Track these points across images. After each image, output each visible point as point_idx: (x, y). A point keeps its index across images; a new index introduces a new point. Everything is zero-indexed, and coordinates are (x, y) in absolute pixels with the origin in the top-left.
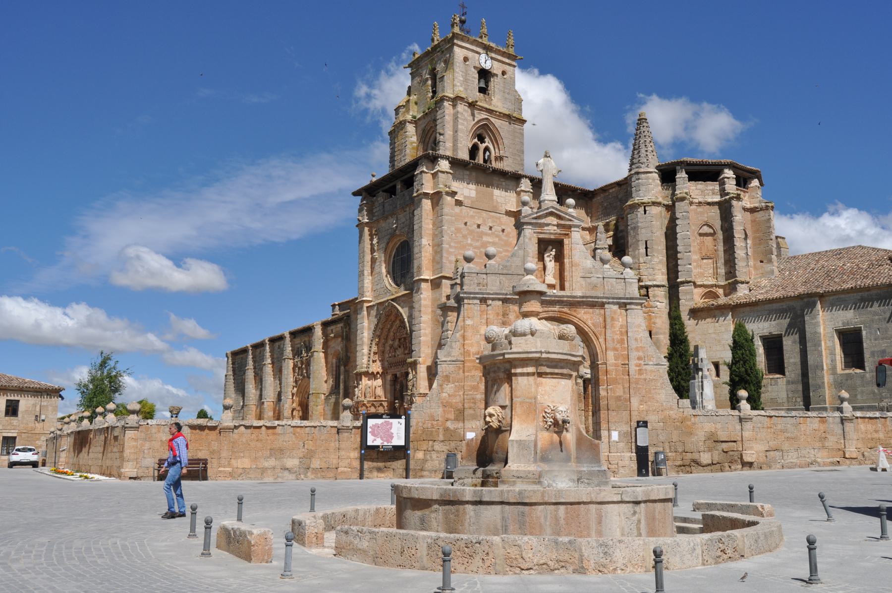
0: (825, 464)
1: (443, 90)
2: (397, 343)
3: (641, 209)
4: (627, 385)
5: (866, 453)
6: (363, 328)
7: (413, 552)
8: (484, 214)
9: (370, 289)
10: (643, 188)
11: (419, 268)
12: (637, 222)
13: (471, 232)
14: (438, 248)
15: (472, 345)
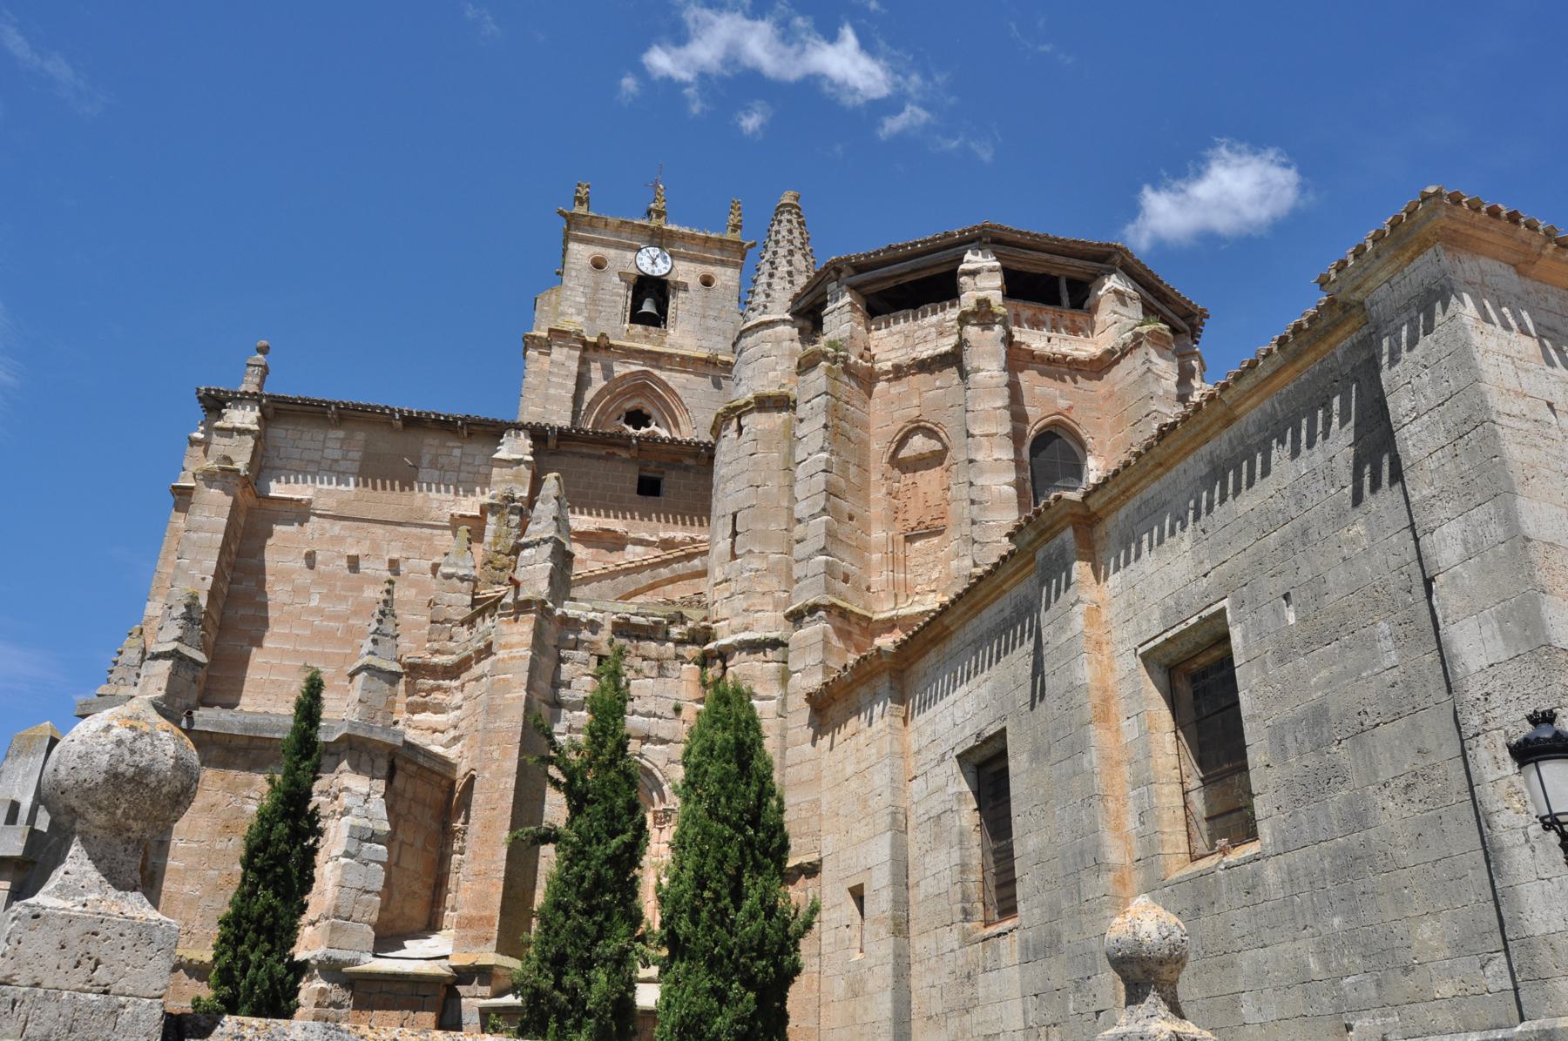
8: (379, 530)
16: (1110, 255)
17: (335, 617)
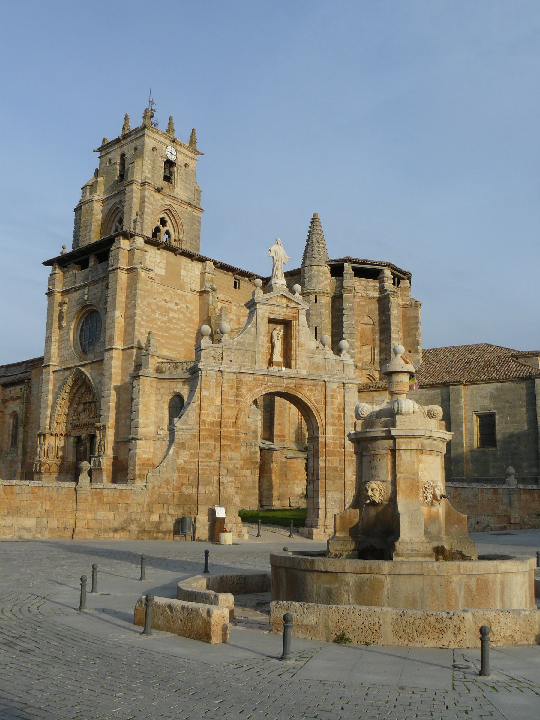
0: (496, 529)
1: (133, 175)
2: (81, 407)
4: (342, 458)
5: (525, 519)
6: (48, 391)
7: (376, 627)
9: (56, 355)
10: (314, 282)
11: (112, 338)
13: (160, 307)
14: (130, 320)
15: (208, 415)
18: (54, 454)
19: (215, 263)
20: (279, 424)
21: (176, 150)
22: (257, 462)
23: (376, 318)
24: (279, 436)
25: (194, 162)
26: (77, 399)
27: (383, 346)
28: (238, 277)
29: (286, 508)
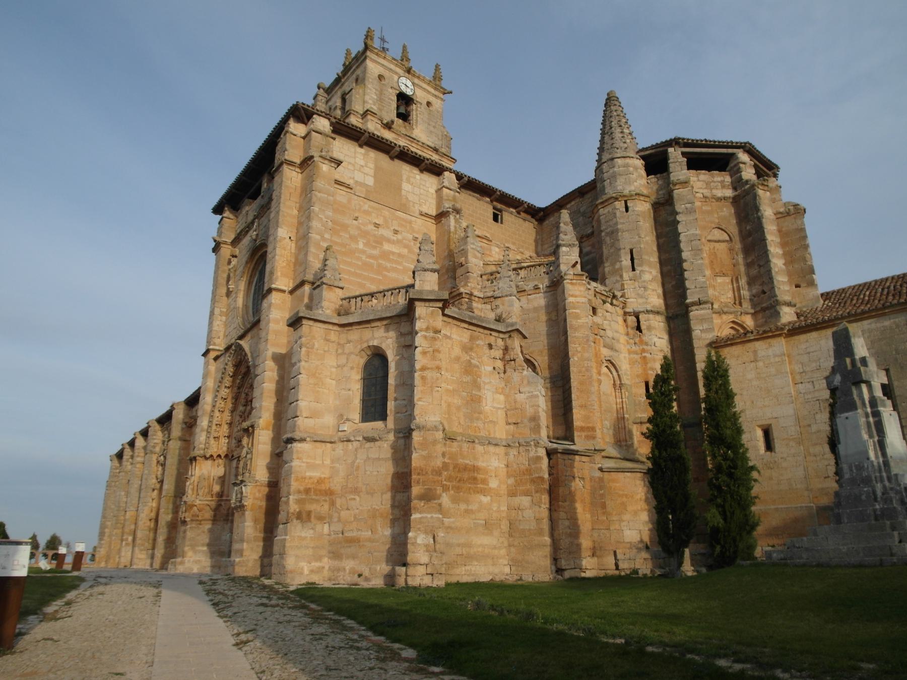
1: (351, 105)
3: (620, 205)
8: (386, 212)
9: (221, 334)
12: (616, 224)
13: (365, 234)
14: (303, 240)
16: (773, 168)
17: (370, 257)
18: (206, 490)
19: (459, 177)
20: (581, 406)
21: (413, 84)
22: (542, 478)
23: (734, 229)
24: (582, 429)
25: (439, 101)
26: (243, 395)
27: (754, 271)
28: (499, 206)
29: (610, 573)
